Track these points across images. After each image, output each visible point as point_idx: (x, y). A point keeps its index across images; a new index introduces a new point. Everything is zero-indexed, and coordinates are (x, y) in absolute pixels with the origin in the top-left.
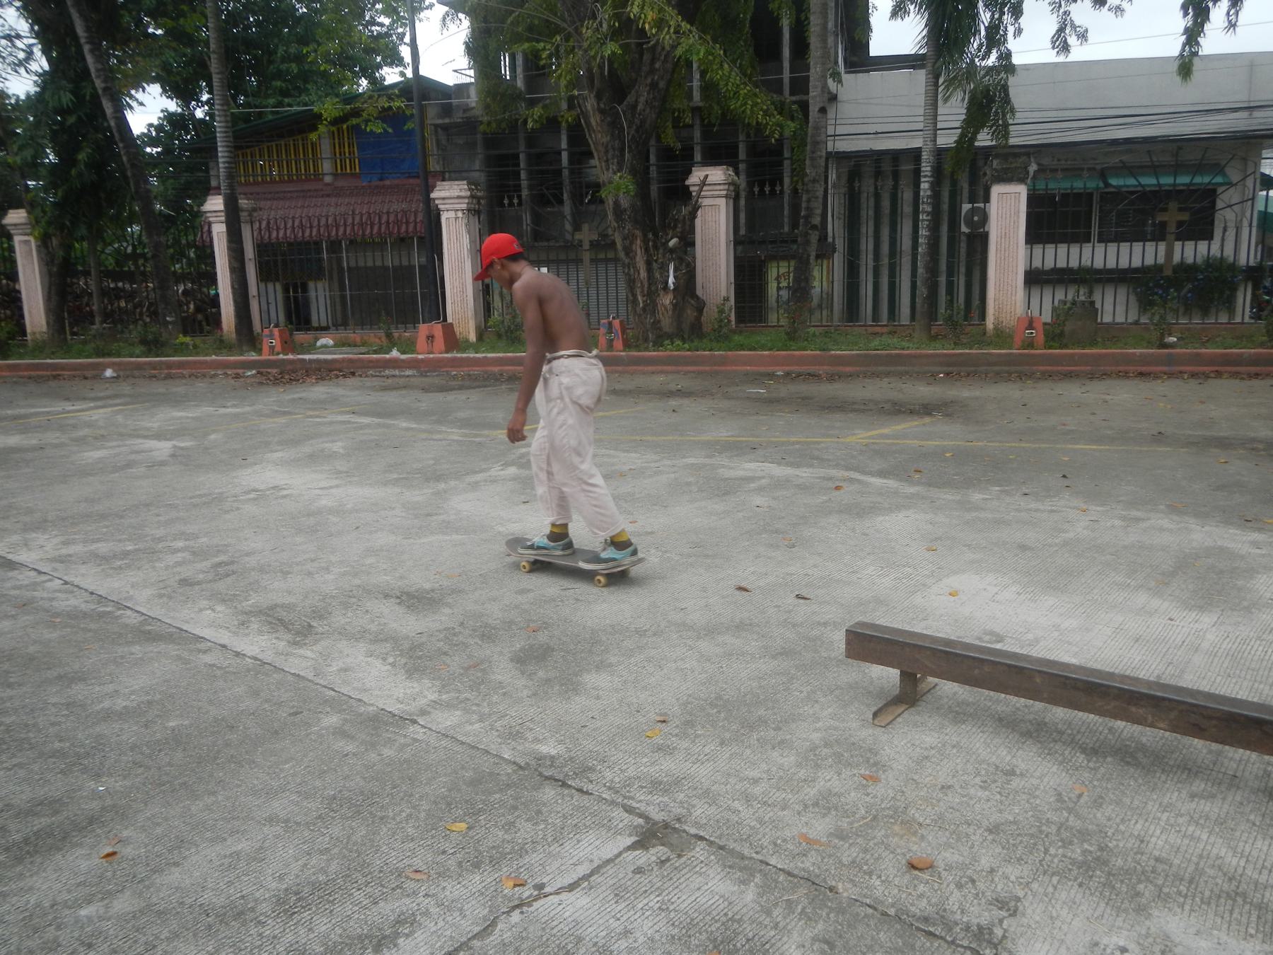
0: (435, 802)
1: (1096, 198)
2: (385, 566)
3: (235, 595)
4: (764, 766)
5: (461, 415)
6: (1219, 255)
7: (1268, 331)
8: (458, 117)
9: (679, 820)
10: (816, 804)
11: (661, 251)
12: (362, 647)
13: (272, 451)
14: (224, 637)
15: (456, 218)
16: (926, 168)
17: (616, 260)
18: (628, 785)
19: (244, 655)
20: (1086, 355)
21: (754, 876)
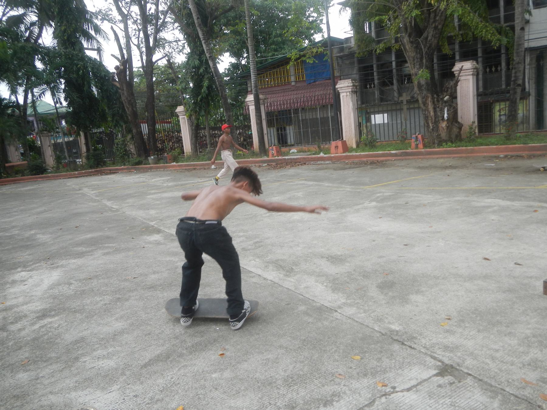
0: (346, 346)
2: (321, 245)
3: (262, 255)
4: (501, 344)
5: (351, 180)
8: (346, 52)
9: (458, 365)
10: (529, 364)
11: (440, 102)
13: (274, 197)
14: (259, 272)
15: (347, 96)
17: (419, 108)
18: (433, 347)
19: (267, 279)
21: (498, 396)
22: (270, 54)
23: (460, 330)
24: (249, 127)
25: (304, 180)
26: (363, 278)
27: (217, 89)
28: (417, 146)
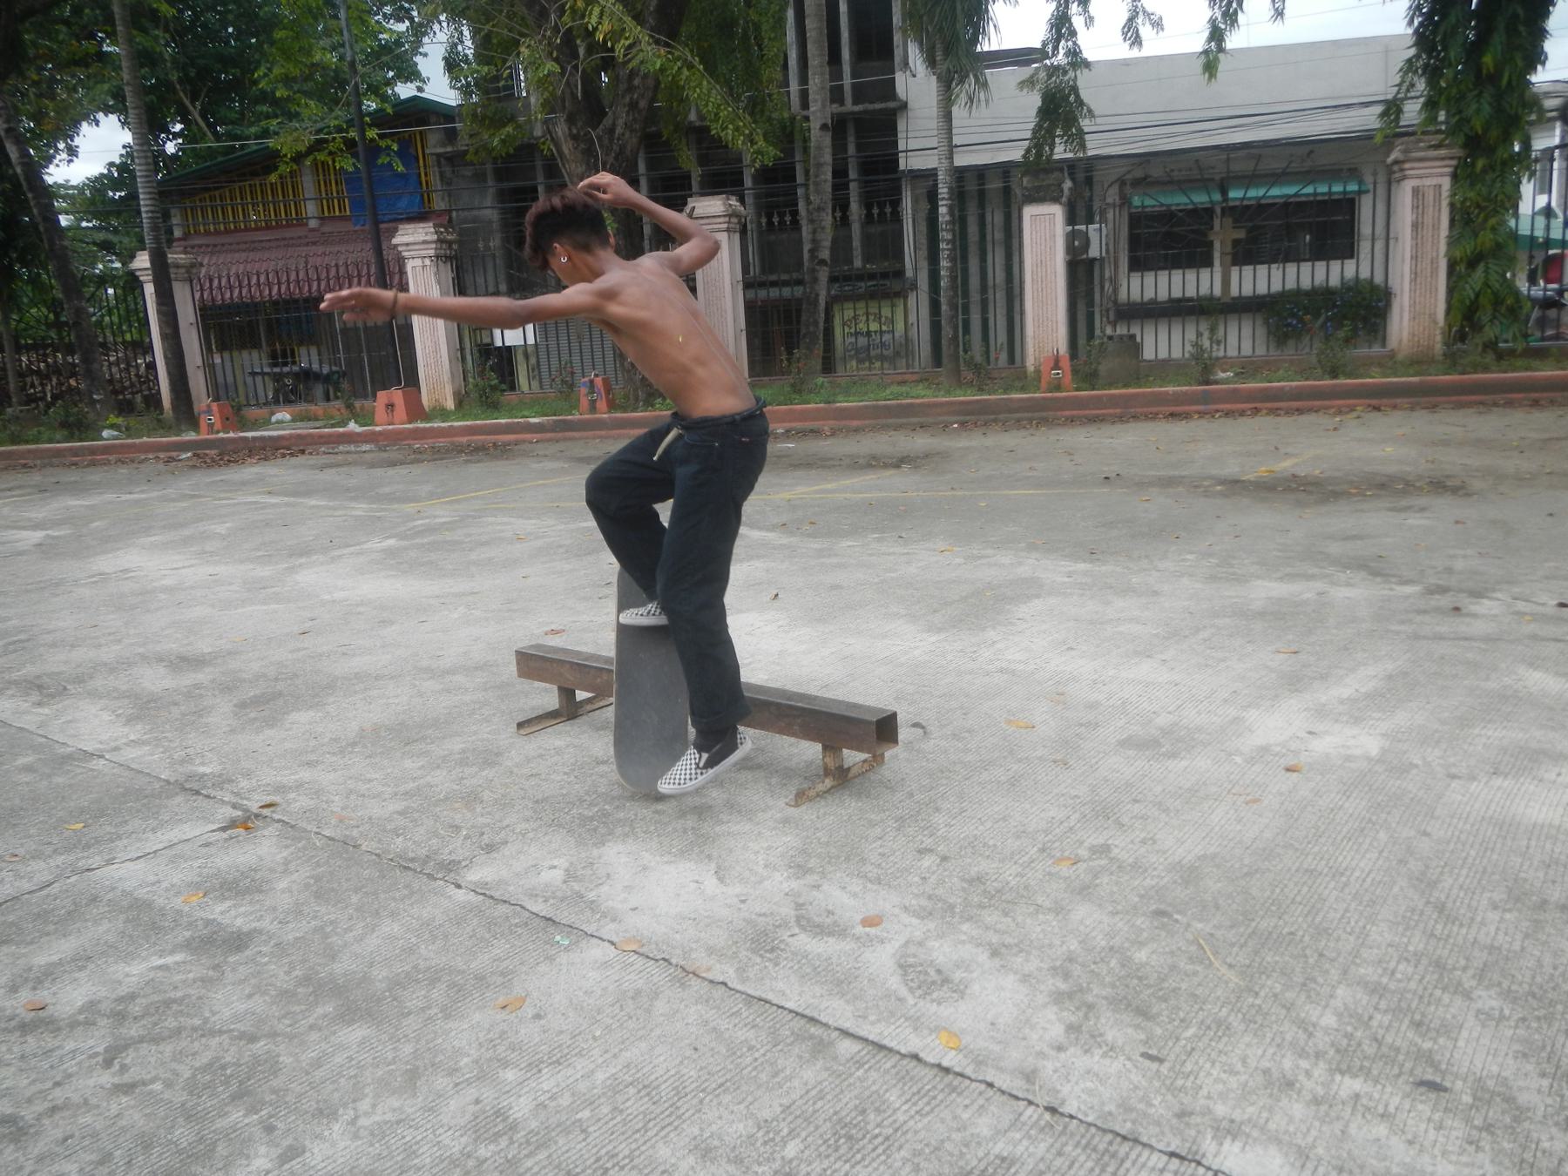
1: (1218, 211)
5: (387, 490)
7: (1319, 361)
10: (406, 793)
15: (423, 267)
16: (943, 191)
20: (1113, 395)
22: (253, 130)
23: (335, 759)
25: (260, 493)
27: (36, 228)
28: (593, 407)
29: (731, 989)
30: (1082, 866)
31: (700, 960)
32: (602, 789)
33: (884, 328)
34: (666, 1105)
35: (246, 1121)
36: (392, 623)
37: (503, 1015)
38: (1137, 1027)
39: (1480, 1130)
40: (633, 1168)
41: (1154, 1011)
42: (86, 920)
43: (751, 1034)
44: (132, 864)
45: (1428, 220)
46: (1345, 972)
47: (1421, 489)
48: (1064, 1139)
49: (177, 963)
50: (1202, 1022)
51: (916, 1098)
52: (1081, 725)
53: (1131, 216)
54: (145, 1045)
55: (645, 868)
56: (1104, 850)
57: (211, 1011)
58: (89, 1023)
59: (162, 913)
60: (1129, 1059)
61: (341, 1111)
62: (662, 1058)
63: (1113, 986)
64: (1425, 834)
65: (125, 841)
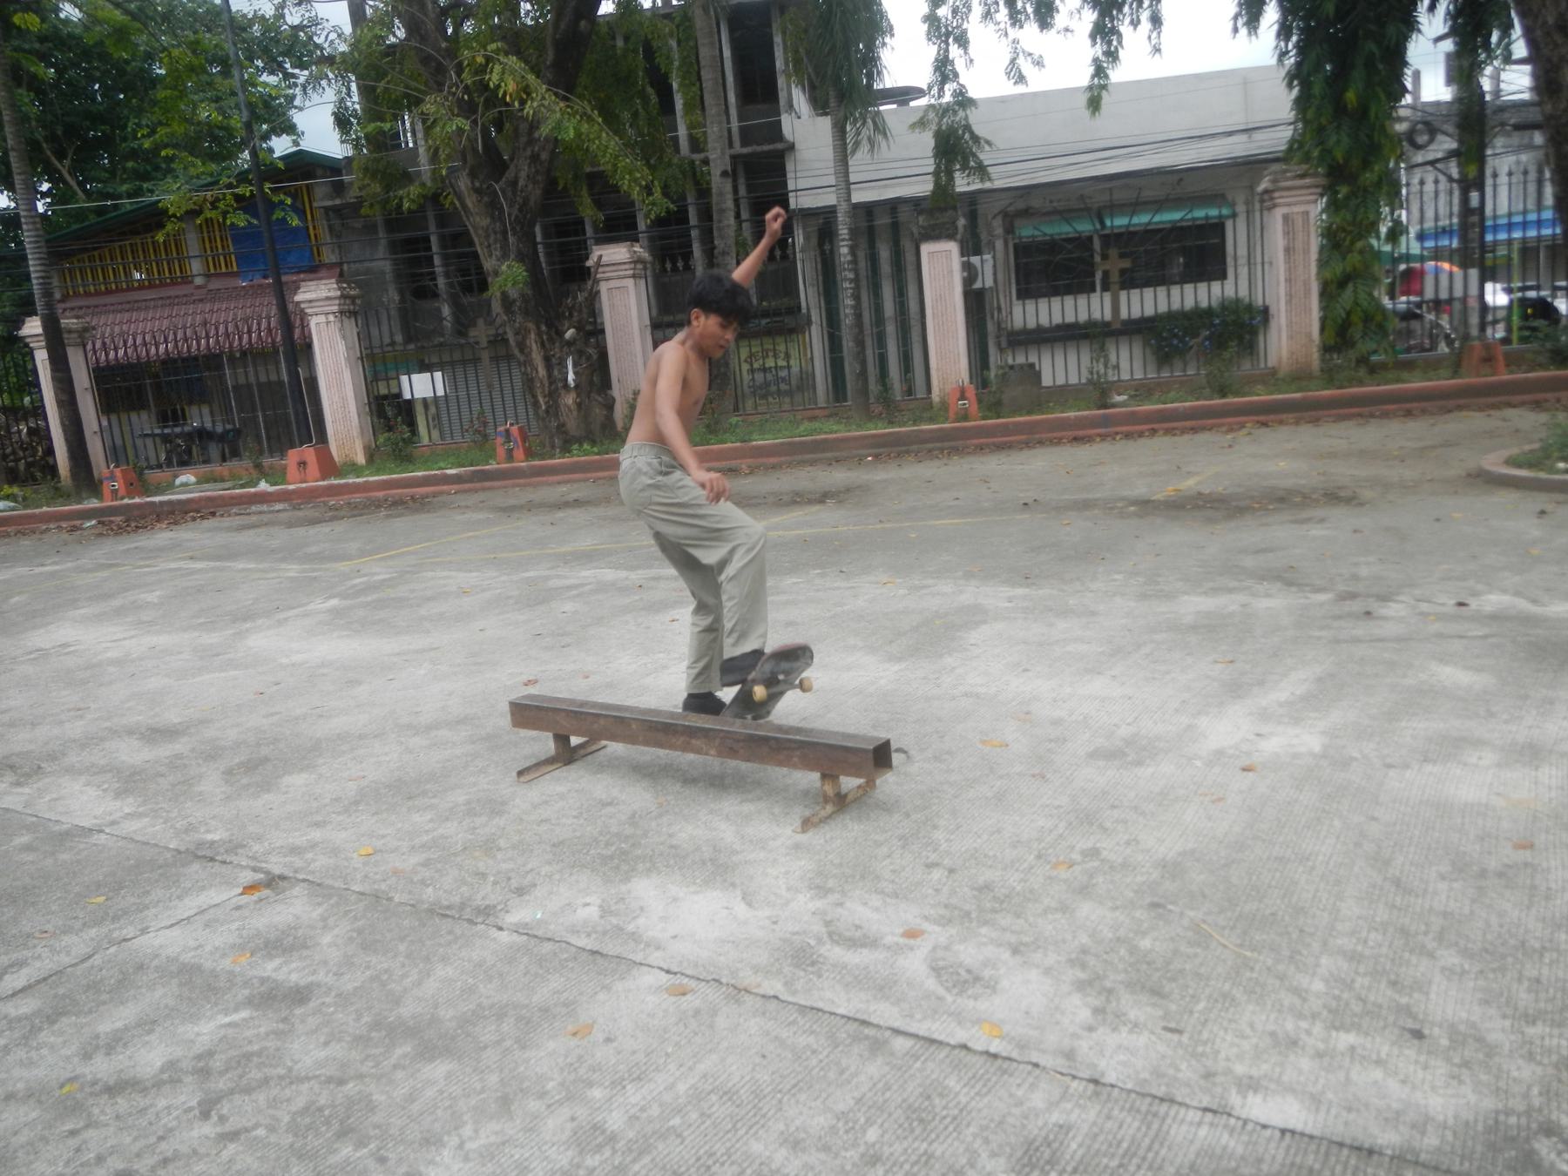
5: (313, 549)
6: (1233, 295)
7: (1208, 382)
8: (351, 195)
10: (423, 846)
11: (557, 344)
12: (83, 779)
15: (328, 323)
16: (843, 232)
20: (1016, 424)
22: (125, 188)
24: (39, 411)
26: (200, 761)
28: (510, 452)
29: (783, 1001)
30: (1077, 868)
31: (748, 978)
32: (614, 829)
33: (781, 363)
34: (749, 1107)
35: (358, 1155)
36: (359, 683)
37: (574, 1042)
38: (1154, 1005)
39: (1460, 1066)
40: (733, 1163)
41: (1167, 989)
42: (140, 987)
43: (811, 1039)
44: (167, 931)
45: (1299, 245)
46: (1325, 944)
47: (1317, 501)
48: (1109, 1105)
49: (244, 1020)
50: (1210, 996)
51: (973, 1082)
52: (1051, 741)
53: (1016, 247)
54: (237, 1096)
55: (675, 899)
56: (1094, 853)
57: (292, 1060)
58: (175, 1081)
59: (214, 974)
60: (1153, 1033)
61: (446, 1138)
62: (734, 1067)
63: (1126, 971)
64: (1374, 819)
65: (154, 911)
